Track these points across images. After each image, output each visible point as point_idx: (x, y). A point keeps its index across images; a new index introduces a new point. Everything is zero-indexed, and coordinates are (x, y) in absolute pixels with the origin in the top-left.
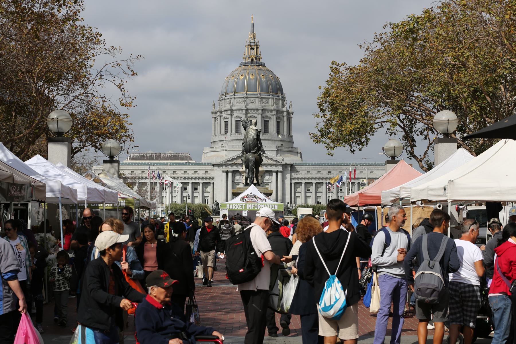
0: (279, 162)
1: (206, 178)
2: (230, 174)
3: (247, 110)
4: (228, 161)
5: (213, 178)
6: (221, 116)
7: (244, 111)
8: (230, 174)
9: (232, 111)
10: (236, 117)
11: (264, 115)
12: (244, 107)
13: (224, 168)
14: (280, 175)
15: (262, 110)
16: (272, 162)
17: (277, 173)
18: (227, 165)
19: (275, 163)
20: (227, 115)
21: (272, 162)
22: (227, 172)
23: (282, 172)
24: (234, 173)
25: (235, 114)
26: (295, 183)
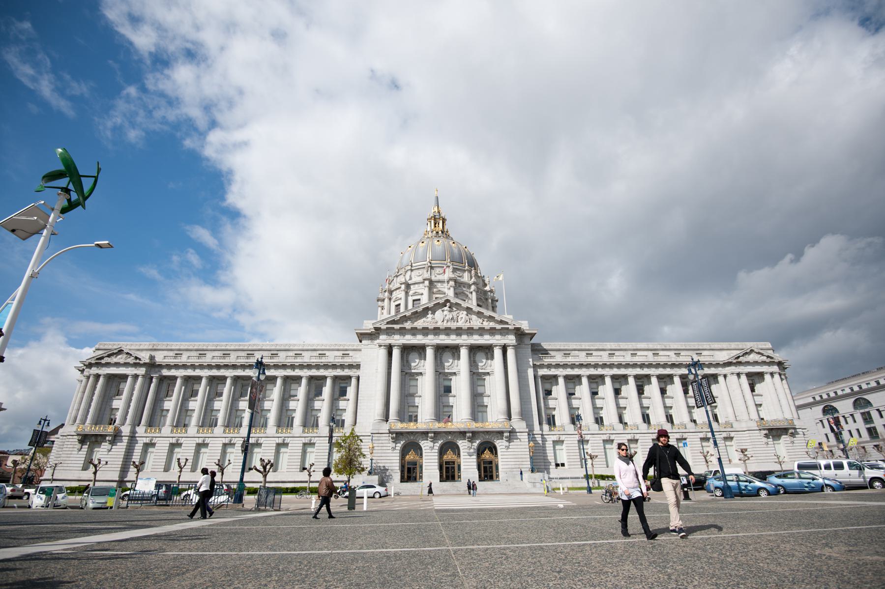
0: (507, 323)
1: (342, 367)
2: (396, 353)
3: (431, 282)
4: (394, 322)
5: (358, 366)
6: (390, 299)
7: (427, 283)
8: (396, 353)
9: (408, 286)
10: (415, 294)
11: (457, 291)
12: (427, 275)
13: (384, 339)
14: (511, 353)
15: (455, 281)
16: (492, 324)
17: (504, 349)
18: (389, 332)
19: (499, 327)
20: (400, 294)
21: (492, 324)
22: (390, 349)
23: (516, 347)
24: (407, 350)
25: (413, 289)
26: (545, 378)
